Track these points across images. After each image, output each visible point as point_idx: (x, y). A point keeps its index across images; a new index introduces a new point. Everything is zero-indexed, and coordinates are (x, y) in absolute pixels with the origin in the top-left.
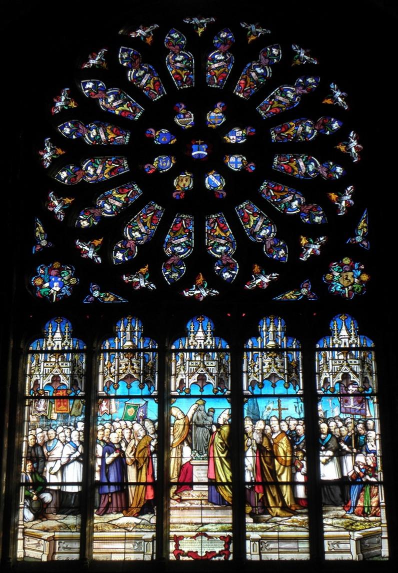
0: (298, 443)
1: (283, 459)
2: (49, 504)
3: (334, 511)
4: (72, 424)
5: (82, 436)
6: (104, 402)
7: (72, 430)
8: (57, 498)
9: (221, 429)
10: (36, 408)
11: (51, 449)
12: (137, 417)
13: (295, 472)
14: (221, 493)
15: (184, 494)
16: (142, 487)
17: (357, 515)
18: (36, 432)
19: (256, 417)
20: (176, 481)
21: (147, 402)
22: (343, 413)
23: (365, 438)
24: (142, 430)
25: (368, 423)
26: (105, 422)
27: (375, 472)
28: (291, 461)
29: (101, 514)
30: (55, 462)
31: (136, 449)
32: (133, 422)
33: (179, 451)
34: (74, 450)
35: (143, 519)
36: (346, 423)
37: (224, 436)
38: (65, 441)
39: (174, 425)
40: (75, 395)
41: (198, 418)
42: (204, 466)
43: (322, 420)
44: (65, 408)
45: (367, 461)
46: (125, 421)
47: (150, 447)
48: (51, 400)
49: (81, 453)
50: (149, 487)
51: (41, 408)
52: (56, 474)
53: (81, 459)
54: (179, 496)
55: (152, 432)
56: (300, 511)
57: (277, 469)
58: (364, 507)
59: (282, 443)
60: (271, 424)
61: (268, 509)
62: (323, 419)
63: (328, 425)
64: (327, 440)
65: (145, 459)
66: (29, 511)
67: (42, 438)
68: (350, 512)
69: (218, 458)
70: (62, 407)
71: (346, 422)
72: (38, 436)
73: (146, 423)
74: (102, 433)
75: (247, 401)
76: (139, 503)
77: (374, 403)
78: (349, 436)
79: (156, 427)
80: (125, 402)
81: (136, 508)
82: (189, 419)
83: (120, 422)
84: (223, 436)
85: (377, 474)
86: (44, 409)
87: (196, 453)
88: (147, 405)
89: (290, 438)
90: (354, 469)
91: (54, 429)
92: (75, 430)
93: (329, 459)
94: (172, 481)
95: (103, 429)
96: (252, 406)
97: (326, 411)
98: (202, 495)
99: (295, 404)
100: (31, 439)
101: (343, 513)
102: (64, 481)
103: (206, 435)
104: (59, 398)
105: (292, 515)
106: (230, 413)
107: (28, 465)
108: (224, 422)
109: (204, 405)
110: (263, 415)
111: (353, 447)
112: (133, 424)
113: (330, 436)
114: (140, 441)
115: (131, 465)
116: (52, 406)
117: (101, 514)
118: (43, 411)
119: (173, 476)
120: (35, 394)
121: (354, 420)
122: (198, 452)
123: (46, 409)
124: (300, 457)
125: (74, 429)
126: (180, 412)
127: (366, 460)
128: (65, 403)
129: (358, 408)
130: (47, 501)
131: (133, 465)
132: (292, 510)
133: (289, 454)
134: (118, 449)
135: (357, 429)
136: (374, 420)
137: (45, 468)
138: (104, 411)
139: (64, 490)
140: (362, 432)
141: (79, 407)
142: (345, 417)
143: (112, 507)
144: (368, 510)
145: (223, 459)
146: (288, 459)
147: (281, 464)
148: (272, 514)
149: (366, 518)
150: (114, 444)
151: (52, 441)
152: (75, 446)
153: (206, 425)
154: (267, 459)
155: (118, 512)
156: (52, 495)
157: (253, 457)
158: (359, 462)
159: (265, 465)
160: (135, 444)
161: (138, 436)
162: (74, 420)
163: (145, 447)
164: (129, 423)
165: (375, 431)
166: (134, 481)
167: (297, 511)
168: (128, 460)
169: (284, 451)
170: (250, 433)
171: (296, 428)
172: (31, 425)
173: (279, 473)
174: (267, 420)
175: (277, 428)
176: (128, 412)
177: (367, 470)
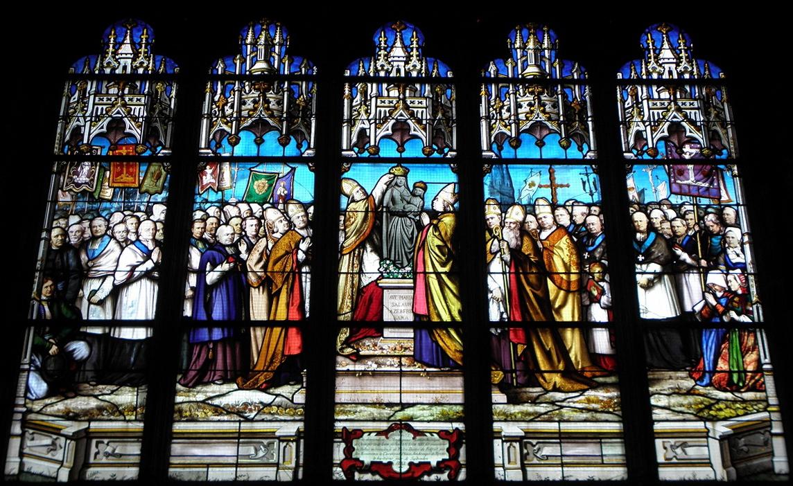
0: (591, 249)
1: (562, 278)
2: (83, 362)
3: (671, 381)
4: (143, 208)
5: (161, 231)
6: (208, 167)
7: (141, 219)
8: (99, 350)
9: (439, 221)
10: (72, 178)
11: (96, 255)
12: (272, 196)
13: (588, 303)
14: (441, 343)
15: (364, 344)
16: (277, 330)
17: (718, 389)
18: (67, 223)
19: (506, 199)
20: (349, 319)
21: (293, 169)
22: (676, 194)
23: (721, 239)
24: (281, 221)
25: (725, 212)
26: (209, 205)
27: (746, 305)
28: (580, 281)
29: (190, 385)
30: (101, 281)
31: (268, 257)
32: (265, 206)
33: (356, 262)
34: (143, 257)
35: (277, 395)
36: (682, 212)
37: (446, 234)
38: (126, 240)
39: (346, 211)
40: (150, 156)
41: (393, 199)
42: (406, 291)
43: (636, 206)
44: (130, 179)
45: (729, 284)
46: (248, 204)
47: (297, 253)
48: (103, 164)
49: (156, 264)
50: (293, 332)
51: (83, 178)
52: (101, 303)
53: (156, 274)
54: (353, 348)
55: (302, 225)
56: (601, 380)
57: (552, 297)
58: (730, 373)
59: (561, 249)
60: (537, 212)
61: (537, 375)
62: (638, 204)
63: (648, 216)
64: (648, 243)
65: (286, 275)
66: (40, 378)
67: (78, 234)
68: (704, 383)
69: (433, 276)
71: (683, 210)
72: (71, 229)
73: (291, 207)
74: (202, 225)
75: (489, 171)
76: (272, 362)
77: (734, 176)
78: (691, 237)
79: (310, 215)
80: (250, 169)
81: (263, 371)
82: (376, 202)
83: (240, 205)
84: (443, 234)
85: (751, 309)
86: (88, 180)
87: (389, 265)
88: (294, 175)
89: (575, 239)
90: (704, 298)
91: (104, 218)
92: (148, 219)
93: (655, 278)
94: (342, 318)
95: (205, 217)
96: (499, 179)
97: (643, 191)
98: (402, 347)
99: (583, 176)
100: (57, 236)
101: (689, 383)
104: (121, 159)
105: (586, 387)
107: (45, 285)
108: (445, 208)
109: (405, 175)
110: (520, 196)
111: (700, 257)
112: (264, 210)
113: (653, 235)
114: (276, 242)
115: (258, 287)
116: (104, 175)
117: (190, 385)
118: (86, 183)
119: (342, 308)
120: (72, 152)
121: (698, 206)
122: (394, 263)
123: (93, 180)
124: (597, 276)
125: (145, 216)
127: (727, 282)
128: (131, 170)
129: (703, 185)
130: (79, 357)
131: (261, 288)
132: (586, 377)
133: (574, 269)
134: (231, 255)
135: (704, 223)
136: (736, 207)
137: (81, 292)
138: (207, 184)
139: (116, 336)
140: (716, 228)
141: (158, 177)
142: (680, 202)
143: (215, 371)
144: (740, 379)
145: (443, 276)
146: (574, 278)
147: (560, 288)
148: (546, 386)
149: (736, 394)
150: (224, 246)
151: (100, 239)
152: (144, 249)
154: (532, 278)
155: (225, 381)
156: (90, 345)
157: (504, 273)
158: (714, 284)
159: (528, 289)
160: (267, 246)
161: (273, 232)
163: (287, 253)
164: (256, 208)
165: (740, 228)
166: (264, 317)
167: (596, 379)
168: (252, 278)
169: (565, 264)
170: (497, 228)
171: (585, 220)
172: (59, 210)
173: (557, 306)
174: (529, 205)
175: (548, 220)
176: (255, 187)
177: (730, 301)
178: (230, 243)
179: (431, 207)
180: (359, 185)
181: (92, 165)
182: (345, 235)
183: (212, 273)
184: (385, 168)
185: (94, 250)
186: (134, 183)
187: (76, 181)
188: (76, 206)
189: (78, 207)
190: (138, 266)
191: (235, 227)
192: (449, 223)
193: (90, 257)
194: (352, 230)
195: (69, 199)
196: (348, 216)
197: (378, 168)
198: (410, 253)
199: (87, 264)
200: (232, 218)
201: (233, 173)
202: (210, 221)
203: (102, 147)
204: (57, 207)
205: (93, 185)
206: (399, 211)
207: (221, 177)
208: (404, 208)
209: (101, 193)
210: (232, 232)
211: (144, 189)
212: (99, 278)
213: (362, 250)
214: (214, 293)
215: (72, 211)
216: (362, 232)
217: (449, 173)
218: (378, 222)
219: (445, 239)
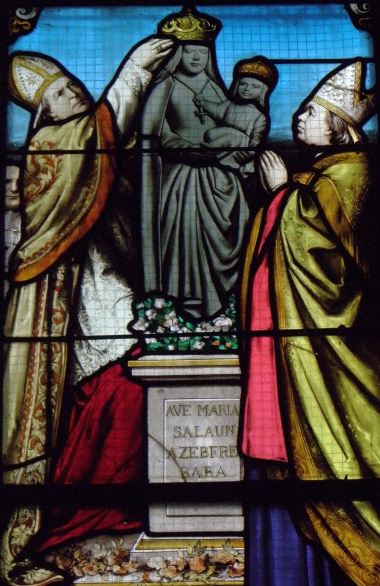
9: (319, 174)
14: (331, 547)
15: (87, 556)
20: (40, 480)
33: (58, 305)
37: (340, 213)
39: (24, 150)
41: (171, 113)
42: (216, 390)
54: (53, 567)
69: (302, 342)
82: (120, 119)
84: (330, 213)
87: (161, 312)
94: (16, 477)
98: (207, 562)
103: (228, 208)
106: (368, 85)
108: (334, 136)
109: (208, 40)
119: (15, 447)
122: (179, 306)
126: (63, 82)
145: (334, 341)
153: (229, 149)
179: (289, 133)
180: (64, 72)
182: (24, 224)
184: (145, 22)
192: (349, 181)
194: (43, 210)
196: (30, 167)
197: (125, 22)
198: (228, 274)
206: (190, 149)
208: (207, 138)
213: (76, 270)
216: (75, 214)
217: (348, 36)
218: (126, 183)
219: (337, 229)
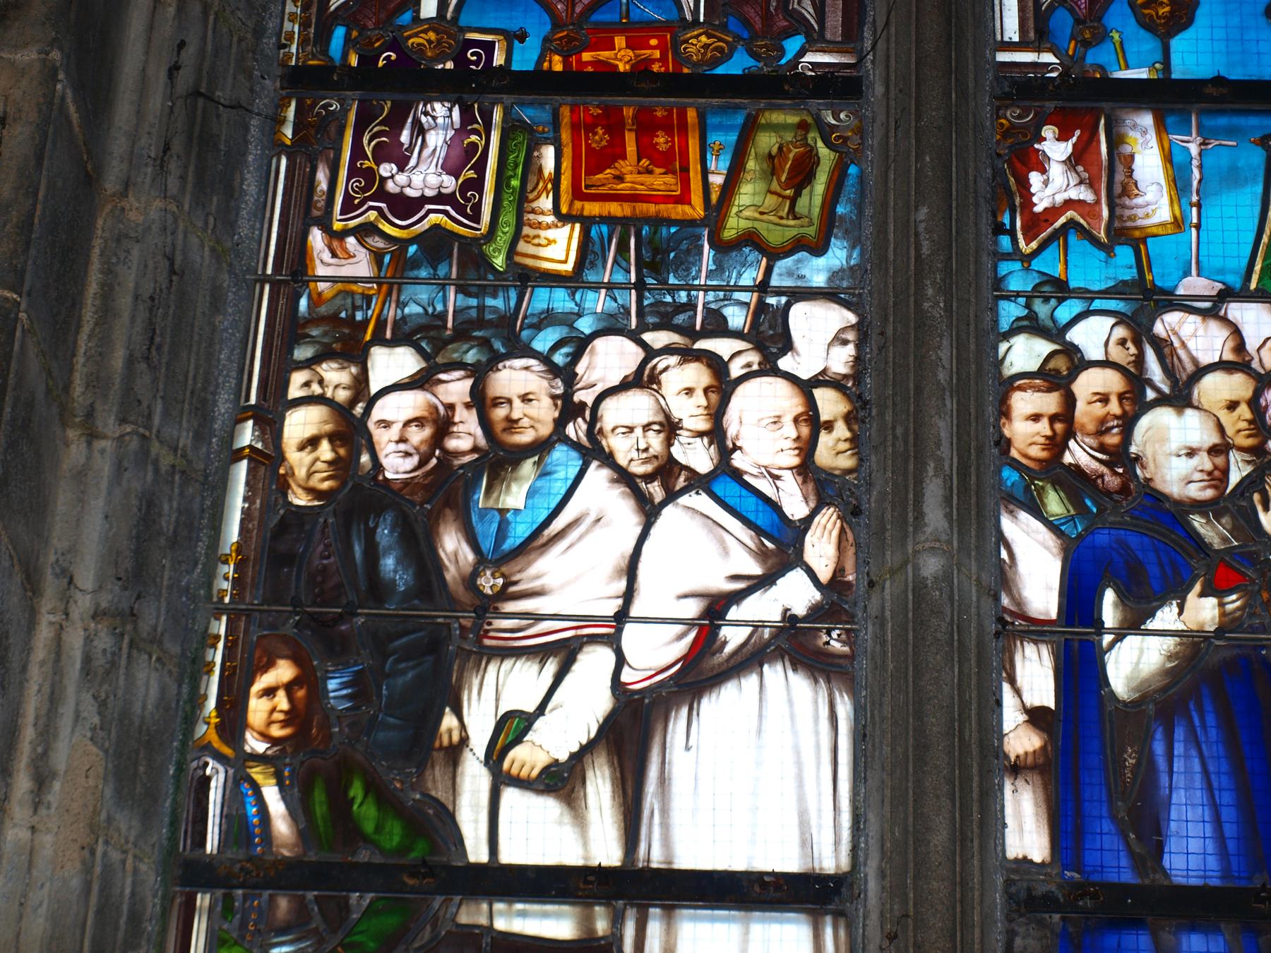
4: (736, 318)
5: (841, 430)
6: (1049, 132)
7: (736, 370)
10: (370, 175)
11: (520, 531)
18: (361, 381)
30: (551, 667)
34: (761, 554)
38: (667, 469)
44: (661, 181)
49: (834, 588)
67: (418, 436)
70: (626, 166)
72: (379, 412)
74: (1050, 402)
83: (1235, 311)
86: (450, 183)
91: (545, 359)
92: (769, 368)
95: (1061, 364)
100: (312, 443)
102: (654, 854)
116: (531, 165)
118: (440, 198)
123: (477, 184)
125: (754, 358)
128: (661, 140)
137: (449, 721)
138: (1053, 212)
141: (803, 174)
151: (528, 467)
162: (749, 277)
172: (313, 320)
178: (1209, 493)
181: (467, 117)
183: (1132, 641)
185: (502, 512)
186: (684, 199)
187: (391, 187)
188: (401, 305)
189: (412, 309)
190: (736, 598)
191: (1225, 417)
193: (487, 545)
195: (361, 266)
199: (470, 581)
200: (1202, 371)
201: (1177, 158)
202: (1088, 384)
203: (515, 37)
204: (303, 303)
205: (477, 208)
207: (1120, 177)
209: (522, 246)
210: (1214, 439)
211: (734, 226)
212: (540, 653)
214: (1159, 748)
215: (381, 324)
